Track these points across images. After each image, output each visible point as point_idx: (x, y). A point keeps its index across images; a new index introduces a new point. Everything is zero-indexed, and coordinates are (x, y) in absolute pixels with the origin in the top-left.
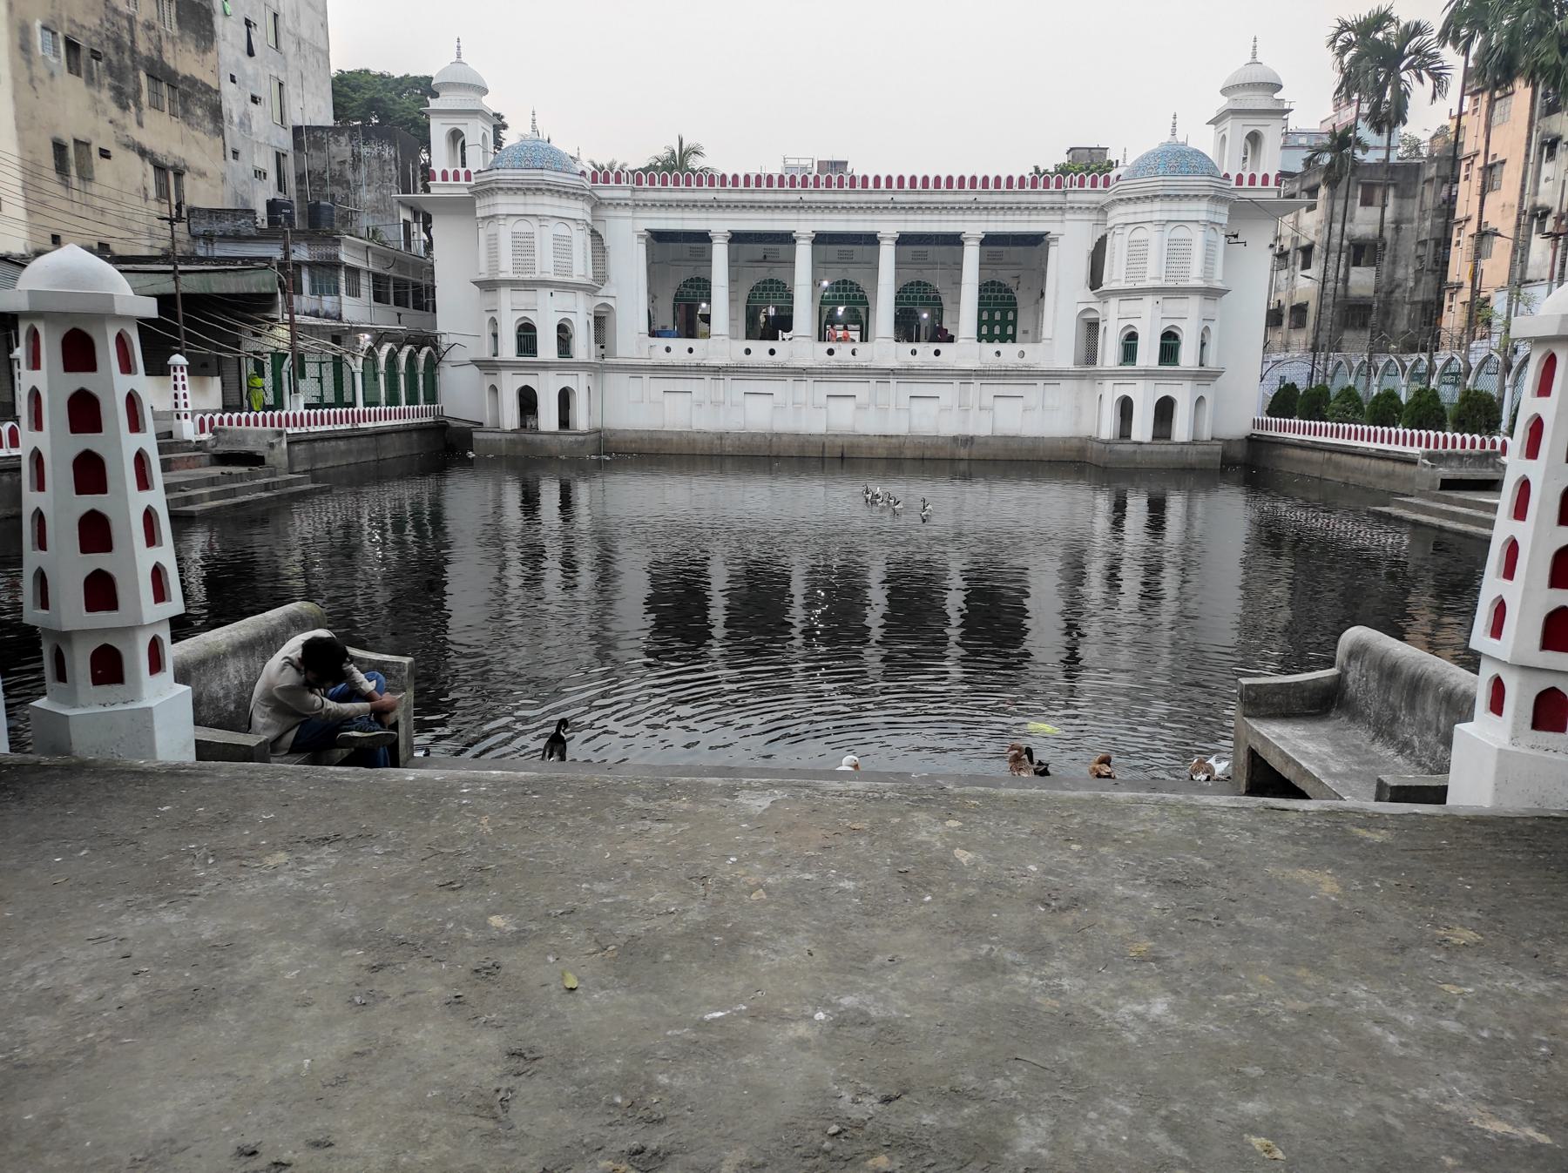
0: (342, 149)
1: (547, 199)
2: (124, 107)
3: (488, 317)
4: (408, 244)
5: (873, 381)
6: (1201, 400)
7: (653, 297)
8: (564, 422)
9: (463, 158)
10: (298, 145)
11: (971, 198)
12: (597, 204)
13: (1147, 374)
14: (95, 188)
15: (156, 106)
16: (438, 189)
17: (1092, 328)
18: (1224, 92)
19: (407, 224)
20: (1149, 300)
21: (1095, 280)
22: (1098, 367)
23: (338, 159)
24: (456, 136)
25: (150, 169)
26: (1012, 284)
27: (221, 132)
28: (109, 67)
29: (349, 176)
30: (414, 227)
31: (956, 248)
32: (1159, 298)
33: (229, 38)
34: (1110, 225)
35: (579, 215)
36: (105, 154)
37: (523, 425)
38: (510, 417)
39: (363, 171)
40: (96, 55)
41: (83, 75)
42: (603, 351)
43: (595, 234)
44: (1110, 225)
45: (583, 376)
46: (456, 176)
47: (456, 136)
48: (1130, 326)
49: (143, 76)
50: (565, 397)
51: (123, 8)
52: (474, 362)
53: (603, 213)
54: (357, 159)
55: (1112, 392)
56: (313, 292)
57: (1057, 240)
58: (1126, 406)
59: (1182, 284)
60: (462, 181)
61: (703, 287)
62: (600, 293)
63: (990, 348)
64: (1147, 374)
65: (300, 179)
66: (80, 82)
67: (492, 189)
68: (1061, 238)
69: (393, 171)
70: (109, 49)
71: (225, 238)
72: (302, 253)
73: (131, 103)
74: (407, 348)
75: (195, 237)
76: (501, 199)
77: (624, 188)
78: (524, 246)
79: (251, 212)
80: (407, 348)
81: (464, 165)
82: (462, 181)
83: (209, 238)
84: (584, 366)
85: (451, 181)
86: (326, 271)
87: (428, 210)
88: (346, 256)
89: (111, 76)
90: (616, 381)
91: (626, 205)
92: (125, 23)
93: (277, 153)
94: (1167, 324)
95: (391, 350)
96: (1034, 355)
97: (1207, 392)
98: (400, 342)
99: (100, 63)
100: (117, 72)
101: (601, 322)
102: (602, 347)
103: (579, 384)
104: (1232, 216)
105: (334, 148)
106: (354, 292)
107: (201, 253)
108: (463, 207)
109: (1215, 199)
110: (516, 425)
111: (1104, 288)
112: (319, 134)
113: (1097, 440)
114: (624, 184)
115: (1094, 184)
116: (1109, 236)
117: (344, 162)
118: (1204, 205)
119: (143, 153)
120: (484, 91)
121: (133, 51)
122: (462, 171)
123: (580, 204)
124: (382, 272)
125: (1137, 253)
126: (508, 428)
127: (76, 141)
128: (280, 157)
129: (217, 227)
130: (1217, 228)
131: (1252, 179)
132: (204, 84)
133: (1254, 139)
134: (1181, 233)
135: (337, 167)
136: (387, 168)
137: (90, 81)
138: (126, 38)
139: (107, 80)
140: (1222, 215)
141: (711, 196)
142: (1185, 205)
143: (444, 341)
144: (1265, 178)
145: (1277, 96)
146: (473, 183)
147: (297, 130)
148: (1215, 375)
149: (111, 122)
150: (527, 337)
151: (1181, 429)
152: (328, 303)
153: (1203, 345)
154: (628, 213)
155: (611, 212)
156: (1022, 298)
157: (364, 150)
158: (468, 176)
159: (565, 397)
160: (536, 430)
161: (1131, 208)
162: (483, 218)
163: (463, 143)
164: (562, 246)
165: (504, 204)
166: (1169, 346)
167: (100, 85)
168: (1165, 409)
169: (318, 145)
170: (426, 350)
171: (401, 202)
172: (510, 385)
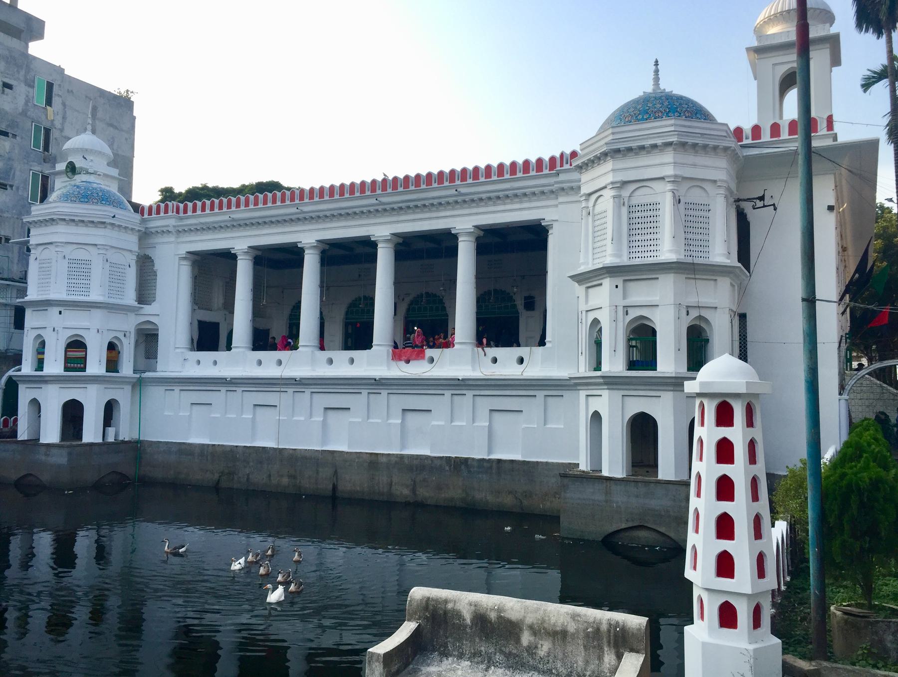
1: (61, 228)
5: (365, 392)
13: (611, 382)
20: (607, 283)
32: (619, 281)
50: (110, 409)
57: (551, 226)
64: (611, 382)
77: (170, 217)
84: (95, 379)
90: (155, 394)
94: (634, 313)
103: (123, 396)
118: (668, 157)
130: (708, 186)
134: (642, 197)
142: (644, 160)
154: (172, 239)
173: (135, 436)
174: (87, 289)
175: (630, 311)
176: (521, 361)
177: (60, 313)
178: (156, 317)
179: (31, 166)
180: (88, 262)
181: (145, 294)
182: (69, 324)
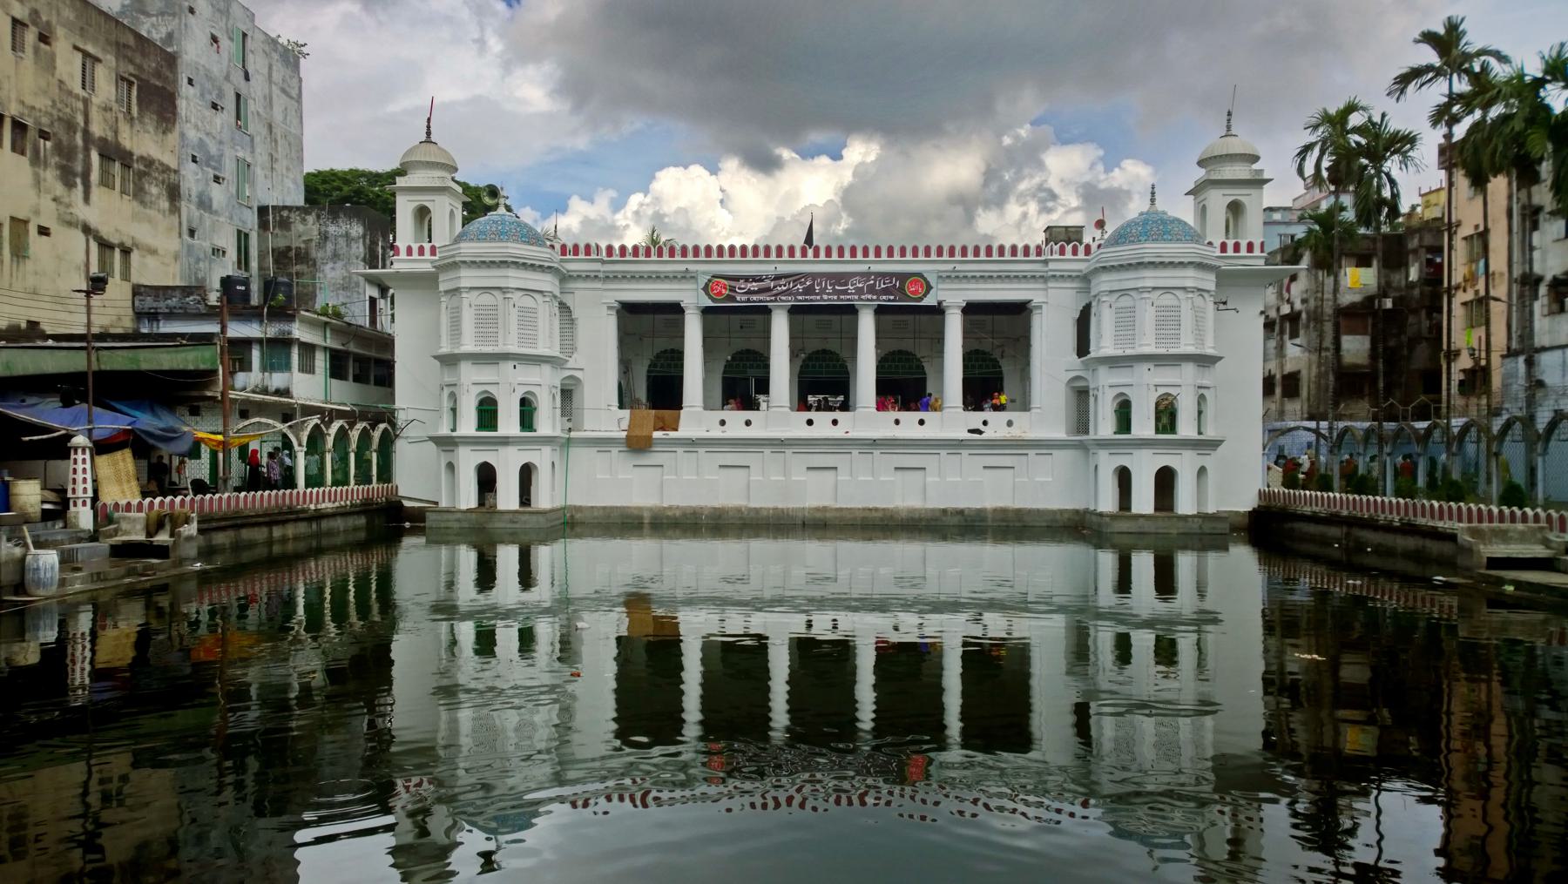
0: (306, 229)
1: (512, 272)
2: (70, 185)
3: (446, 392)
4: (373, 321)
6: (1202, 471)
7: (625, 366)
8: (525, 496)
9: (430, 230)
10: (263, 225)
11: (950, 267)
12: (565, 278)
13: (1144, 443)
14: (29, 266)
15: (106, 182)
16: (401, 264)
17: (1081, 395)
18: (1201, 163)
19: (373, 301)
21: (1083, 348)
22: (1092, 436)
23: (305, 238)
24: (422, 213)
25: (94, 246)
26: (996, 354)
27: (175, 209)
28: (59, 149)
29: (313, 253)
30: (381, 304)
31: (938, 317)
32: (1151, 366)
33: (193, 121)
34: (1093, 293)
35: (546, 287)
36: (43, 231)
37: (481, 503)
38: (468, 497)
39: (330, 247)
40: (44, 135)
41: (28, 153)
42: (569, 425)
43: (564, 308)
44: (1093, 293)
45: (547, 450)
46: (421, 251)
47: (422, 213)
48: (1122, 394)
49: (95, 157)
50: (527, 473)
51: (78, 90)
52: (432, 439)
53: (572, 285)
54: (324, 237)
55: (1108, 464)
56: (264, 369)
58: (1124, 477)
59: (1172, 351)
60: (427, 256)
61: (676, 357)
62: (569, 365)
63: (975, 418)
65: (262, 256)
66: (24, 161)
67: (455, 263)
68: (1044, 306)
69: (359, 249)
70: (59, 129)
71: (171, 315)
72: (251, 330)
73: (79, 181)
74: (360, 426)
75: (139, 315)
76: (464, 272)
78: (488, 322)
79: (198, 289)
80: (360, 426)
81: (430, 241)
82: (427, 256)
83: (153, 316)
85: (415, 256)
86: (278, 349)
87: (388, 283)
88: (299, 332)
89: (59, 155)
91: (596, 277)
92: (80, 105)
93: (239, 232)
94: (1162, 391)
95: (342, 427)
96: (1024, 426)
97: (1210, 461)
98: (351, 418)
99: (49, 144)
100: (66, 152)
101: (567, 394)
102: (569, 420)
104: (1217, 285)
105: (298, 227)
106: (308, 368)
107: (145, 330)
108: (425, 282)
109: (1201, 266)
110: (473, 504)
111: (1092, 355)
112: (285, 213)
113: (1094, 513)
114: (594, 256)
115: (1075, 252)
116: (1094, 304)
117: (311, 240)
119: (87, 229)
120: (456, 170)
121: (86, 132)
122: (427, 246)
123: (548, 277)
124: (340, 347)
125: (1127, 322)
126: (463, 507)
127: (13, 219)
128: (242, 238)
129: (162, 306)
130: (1206, 295)
131: (1237, 248)
132: (162, 164)
133: (1235, 208)
135: (303, 246)
136: (354, 245)
137: (36, 160)
138: (80, 119)
139: (54, 160)
140: (1209, 280)
141: (682, 268)
143: (401, 418)
144: (1250, 247)
145: (1255, 166)
146: (437, 258)
147: (263, 211)
148: (1214, 444)
149: (55, 200)
150: (487, 413)
151: (1185, 504)
152: (277, 380)
153: (1200, 413)
155: (580, 285)
156: (1007, 368)
157: (332, 229)
158: (433, 251)
159: (527, 473)
160: (493, 510)
161: (1114, 276)
162: (447, 292)
163: (430, 221)
164: (527, 319)
165: (468, 278)
166: (1166, 416)
167: (46, 165)
168: (1165, 481)
169: (284, 224)
170: (382, 426)
171: (371, 280)
172: (468, 462)
173: (558, 503)
174: (534, 344)
175: (1159, 388)
176: (1010, 423)
177: (515, 367)
178: (581, 372)
179: (236, 151)
180: (534, 311)
181: (569, 344)
182: (521, 379)
